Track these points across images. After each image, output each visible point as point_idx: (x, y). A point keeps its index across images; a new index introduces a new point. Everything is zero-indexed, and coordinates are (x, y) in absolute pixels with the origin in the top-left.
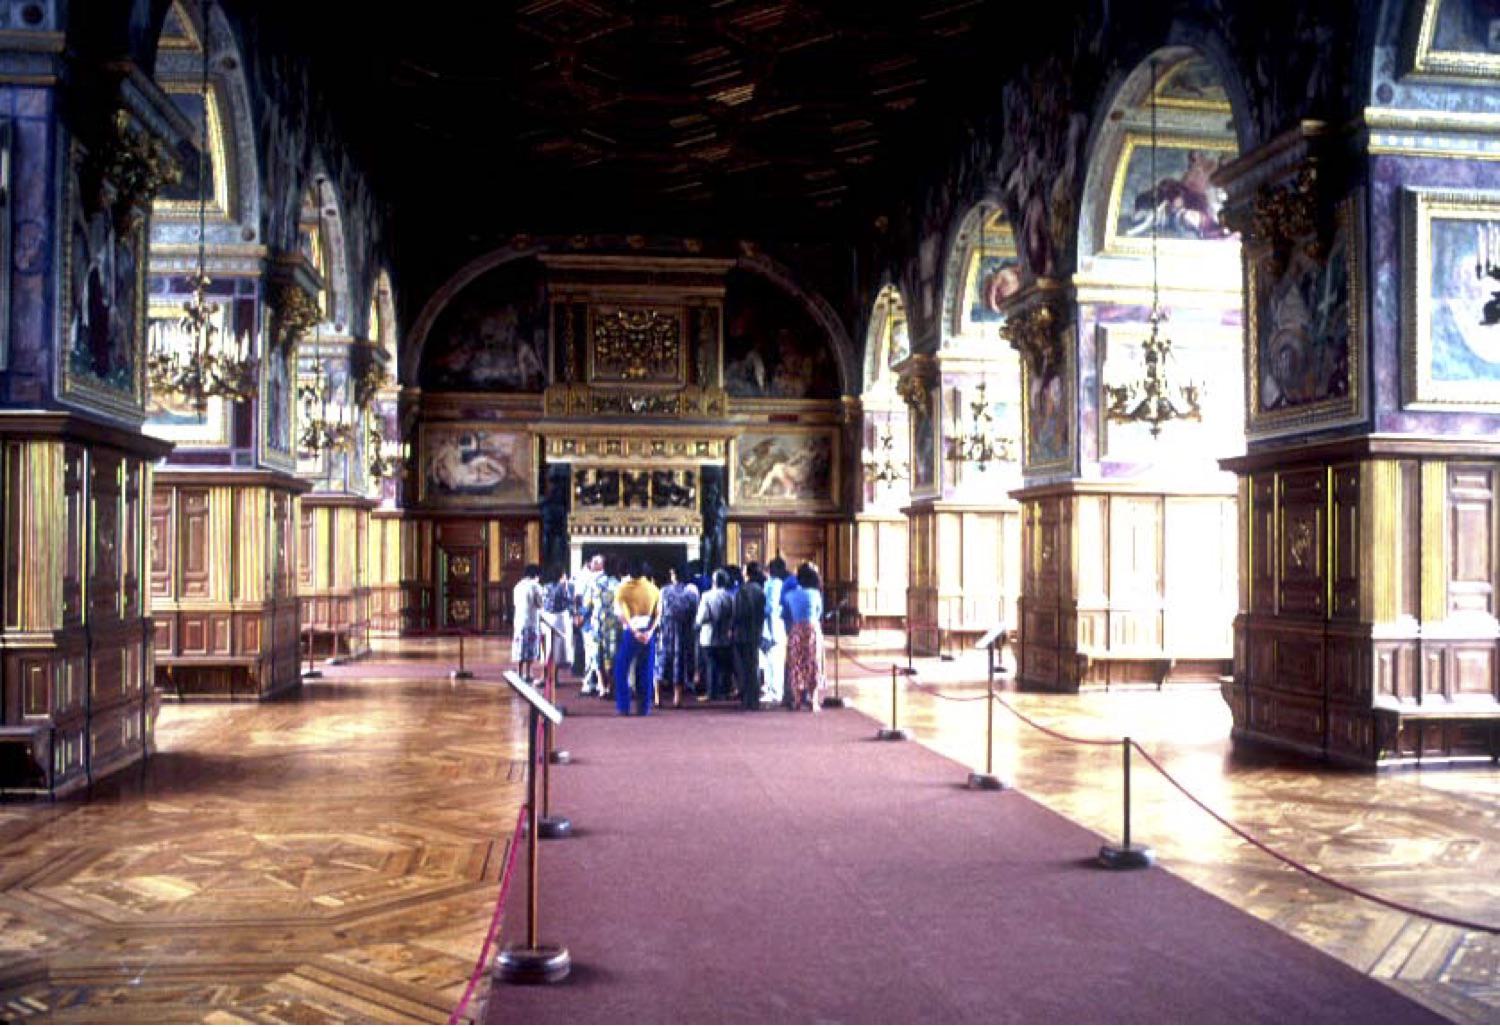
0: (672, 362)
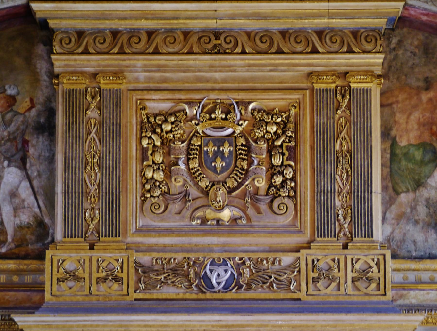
0: (284, 193)
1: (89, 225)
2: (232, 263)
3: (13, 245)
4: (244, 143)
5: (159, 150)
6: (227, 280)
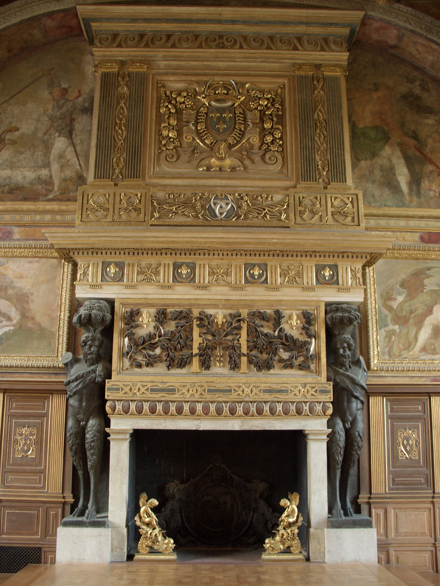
1: (115, 170)
2: (232, 198)
3: (58, 193)
4: (242, 112)
5: (174, 115)
6: (228, 212)
